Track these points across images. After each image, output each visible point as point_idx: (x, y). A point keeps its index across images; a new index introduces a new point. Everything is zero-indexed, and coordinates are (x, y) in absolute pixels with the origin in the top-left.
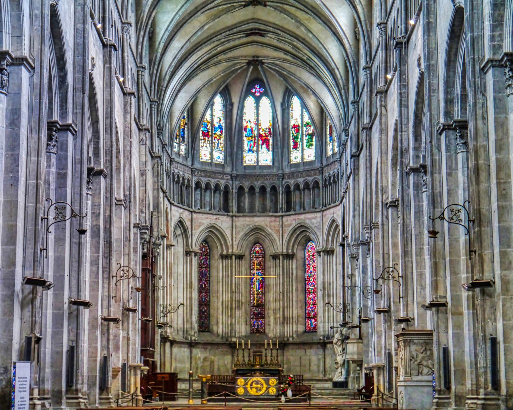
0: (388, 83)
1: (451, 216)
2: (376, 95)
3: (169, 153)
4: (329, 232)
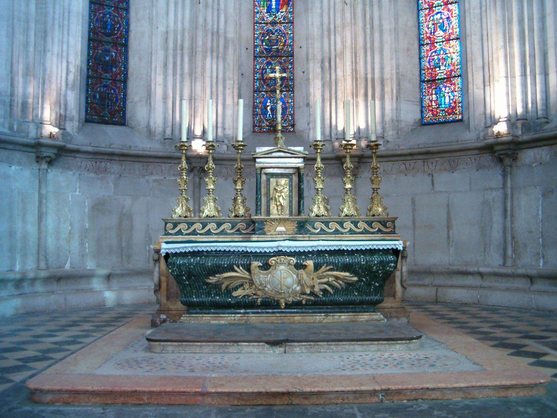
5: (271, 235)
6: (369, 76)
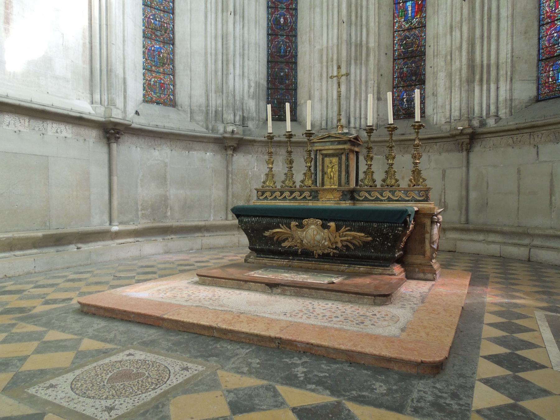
5: (322, 201)
6: (485, 62)
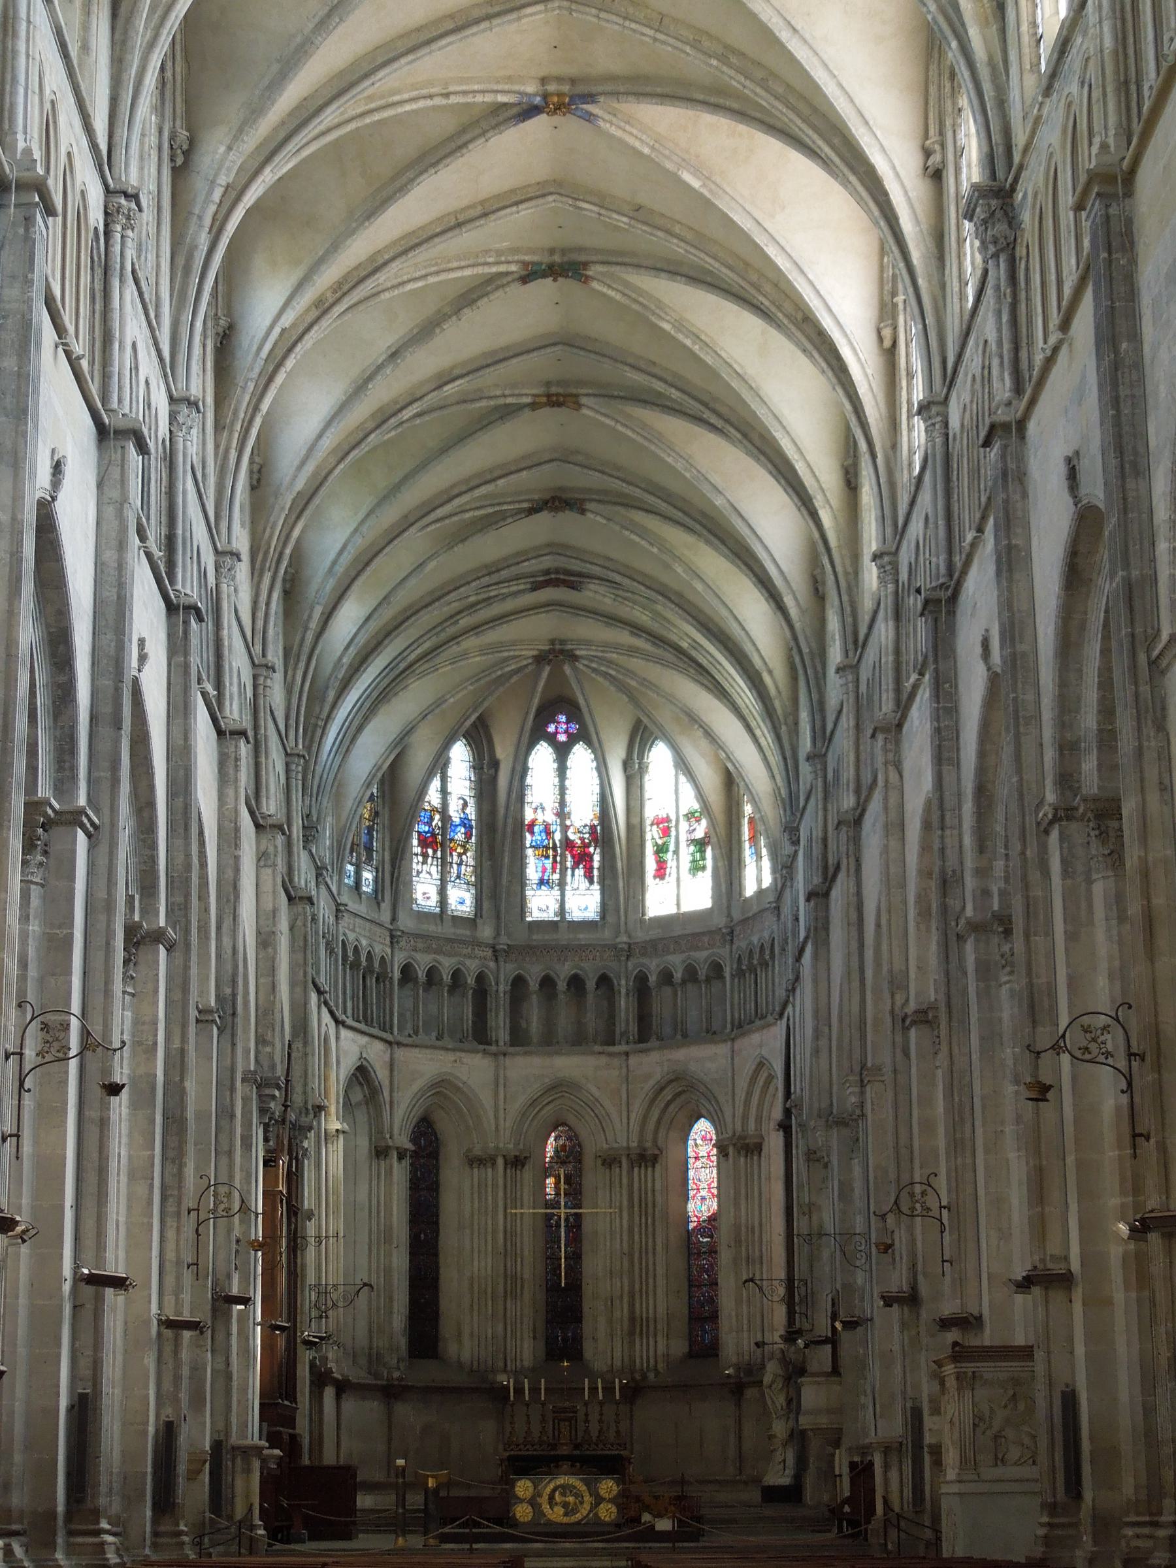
0: (903, 705)
1: (1084, 1043)
2: (873, 736)
3: (334, 889)
4: (749, 1094)
6: (644, 1315)
